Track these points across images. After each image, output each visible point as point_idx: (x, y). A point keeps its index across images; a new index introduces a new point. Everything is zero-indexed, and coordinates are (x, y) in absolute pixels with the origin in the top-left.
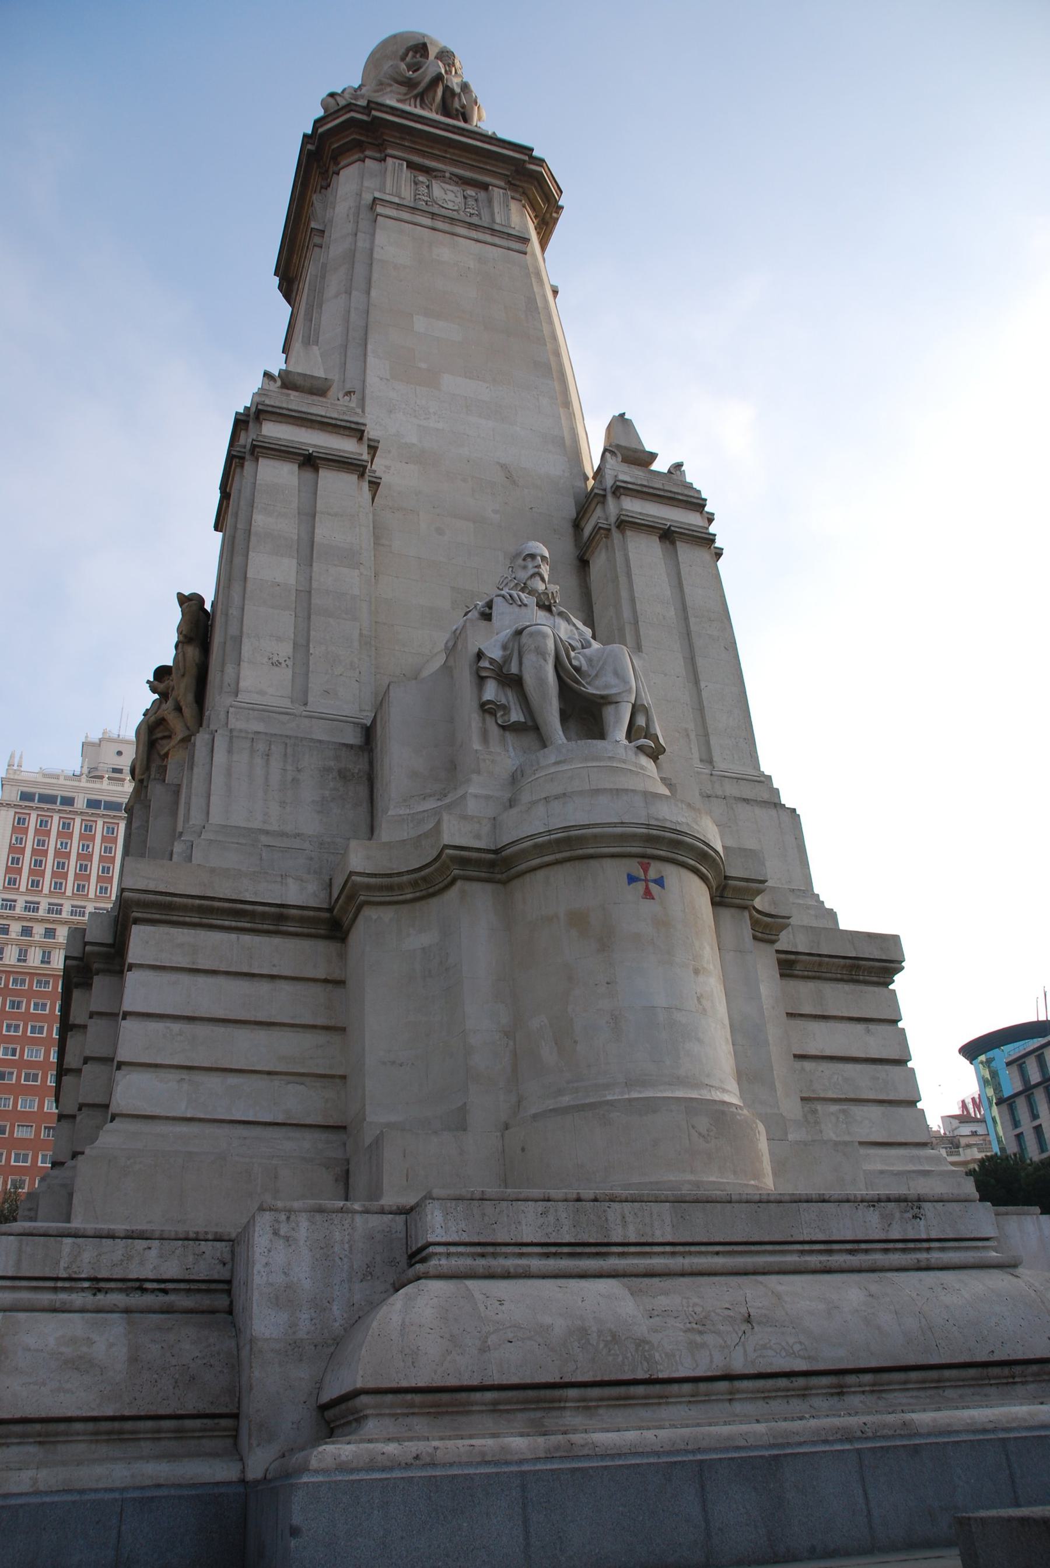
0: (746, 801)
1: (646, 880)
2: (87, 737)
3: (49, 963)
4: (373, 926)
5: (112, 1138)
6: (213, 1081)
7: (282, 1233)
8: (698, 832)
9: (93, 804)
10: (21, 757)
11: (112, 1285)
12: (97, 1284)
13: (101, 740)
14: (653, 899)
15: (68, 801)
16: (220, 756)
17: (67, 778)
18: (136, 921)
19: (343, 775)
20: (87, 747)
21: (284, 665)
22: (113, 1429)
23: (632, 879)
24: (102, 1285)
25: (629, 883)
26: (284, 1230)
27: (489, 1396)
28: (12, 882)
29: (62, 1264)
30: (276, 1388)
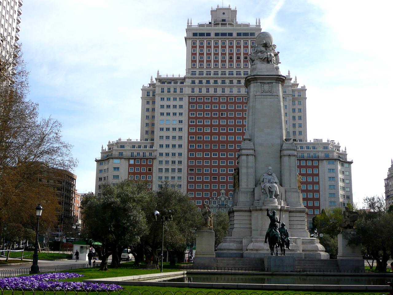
2: (212, 8)
3: (209, 92)
4: (253, 212)
5: (234, 230)
9: (217, 34)
10: (191, 20)
12: (234, 241)
13: (217, 9)
15: (209, 34)
16: (240, 194)
17: (207, 26)
19: (252, 195)
20: (213, 12)
22: (235, 250)
28: (194, 65)
30: (244, 248)
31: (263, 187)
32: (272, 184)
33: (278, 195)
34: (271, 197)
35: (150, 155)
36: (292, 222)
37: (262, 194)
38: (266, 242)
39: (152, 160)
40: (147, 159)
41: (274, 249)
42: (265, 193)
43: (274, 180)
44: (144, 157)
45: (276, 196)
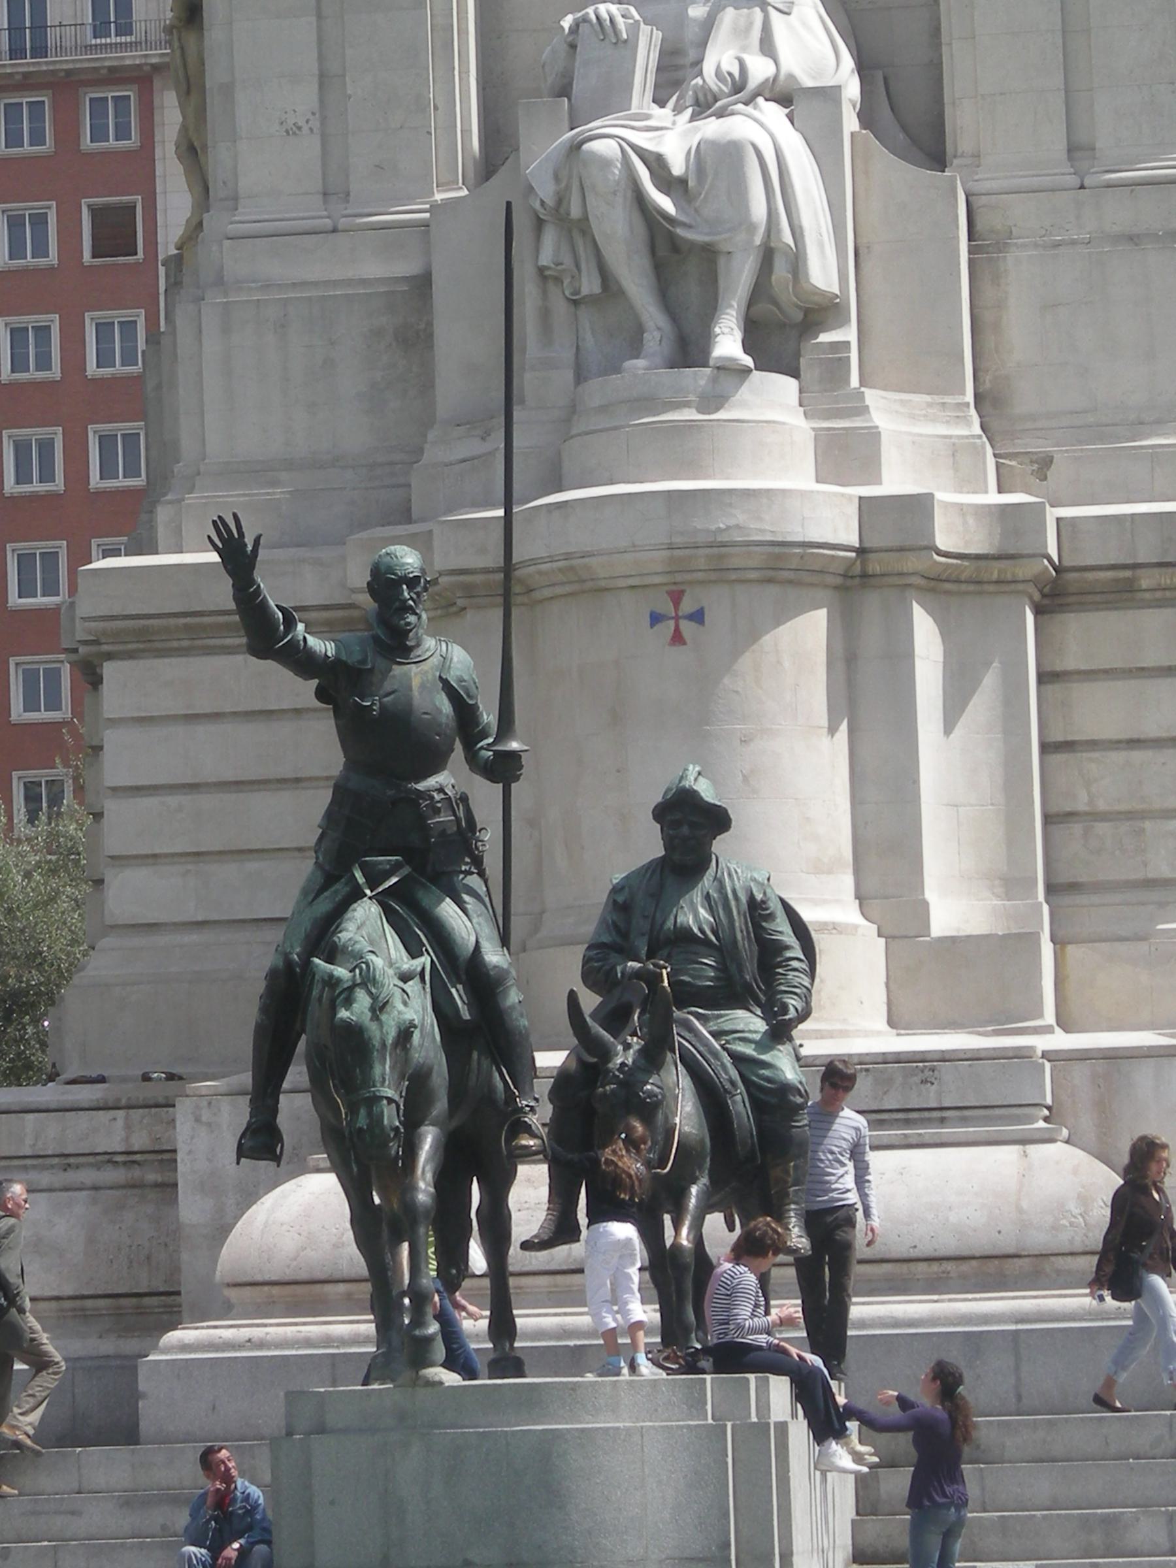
0: (1133, 239)
1: (677, 618)
6: (229, 871)
7: (204, 1119)
8: (762, 531)
11: (81, 1160)
12: (66, 1160)
14: (684, 643)
16: (212, 347)
18: (110, 656)
21: (305, 129)
23: (656, 619)
24: (72, 1160)
25: (652, 626)
26: (206, 1116)
27: (342, 1288)
29: (29, 1141)
31: (546, 191)
32: (711, 128)
33: (820, 312)
34: (690, 349)
35: (100, 29)
36: (1102, 783)
37: (545, 315)
38: (262, 1143)
39: (131, 93)
40: (65, 85)
41: (516, 1257)
42: (590, 285)
43: (767, 46)
44: (27, 64)
45: (785, 333)
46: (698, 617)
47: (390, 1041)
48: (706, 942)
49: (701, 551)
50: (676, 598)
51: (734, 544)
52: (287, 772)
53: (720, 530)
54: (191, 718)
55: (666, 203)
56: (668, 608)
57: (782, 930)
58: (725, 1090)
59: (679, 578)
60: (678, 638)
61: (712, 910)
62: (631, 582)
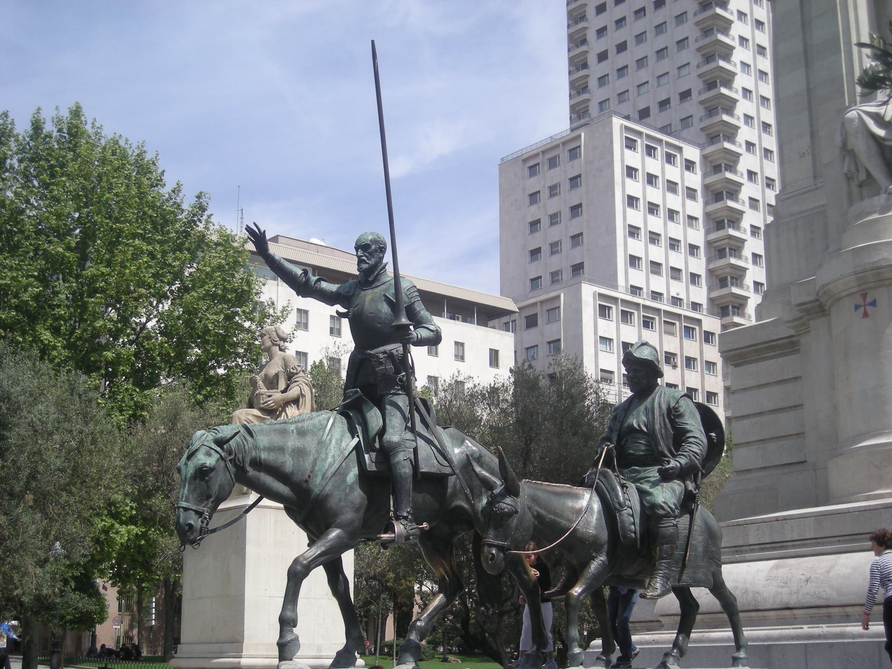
1: (865, 305)
23: (857, 307)
42: (862, 176)
46: (874, 303)
47: (189, 475)
48: (641, 431)
49: (868, 273)
50: (864, 296)
51: (883, 267)
52: (791, 403)
53: (876, 262)
54: (760, 386)
55: (881, 133)
56: (860, 301)
57: (693, 423)
58: (616, 509)
59: (863, 287)
60: (866, 315)
61: (647, 416)
62: (847, 293)
